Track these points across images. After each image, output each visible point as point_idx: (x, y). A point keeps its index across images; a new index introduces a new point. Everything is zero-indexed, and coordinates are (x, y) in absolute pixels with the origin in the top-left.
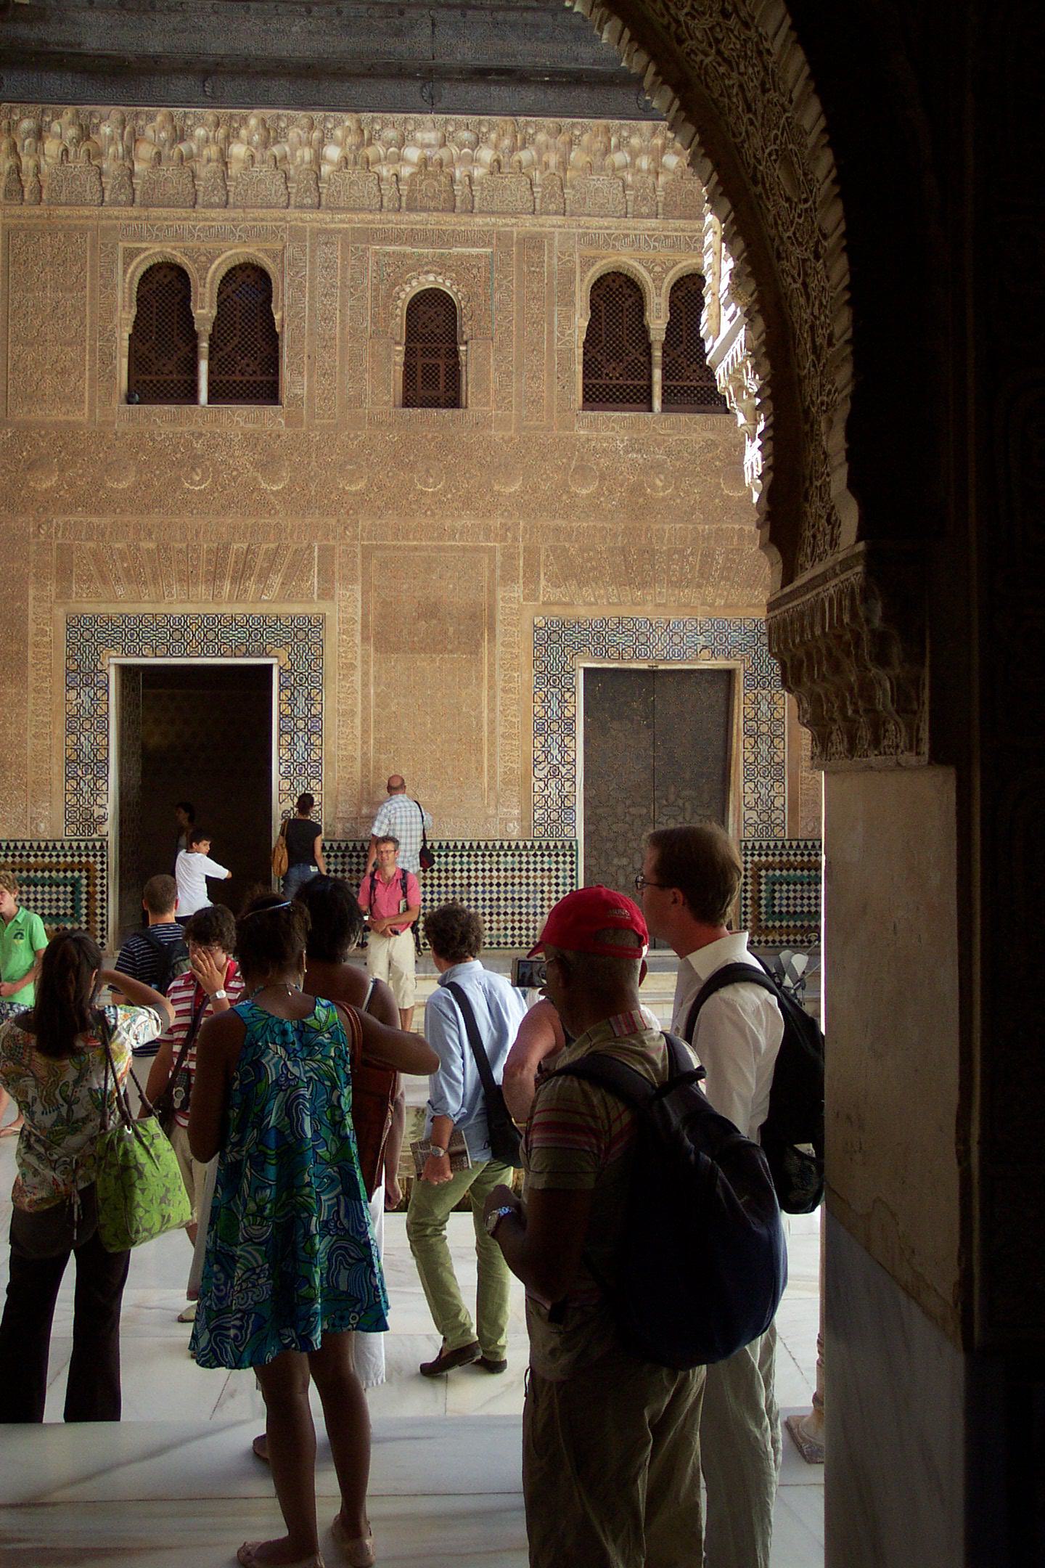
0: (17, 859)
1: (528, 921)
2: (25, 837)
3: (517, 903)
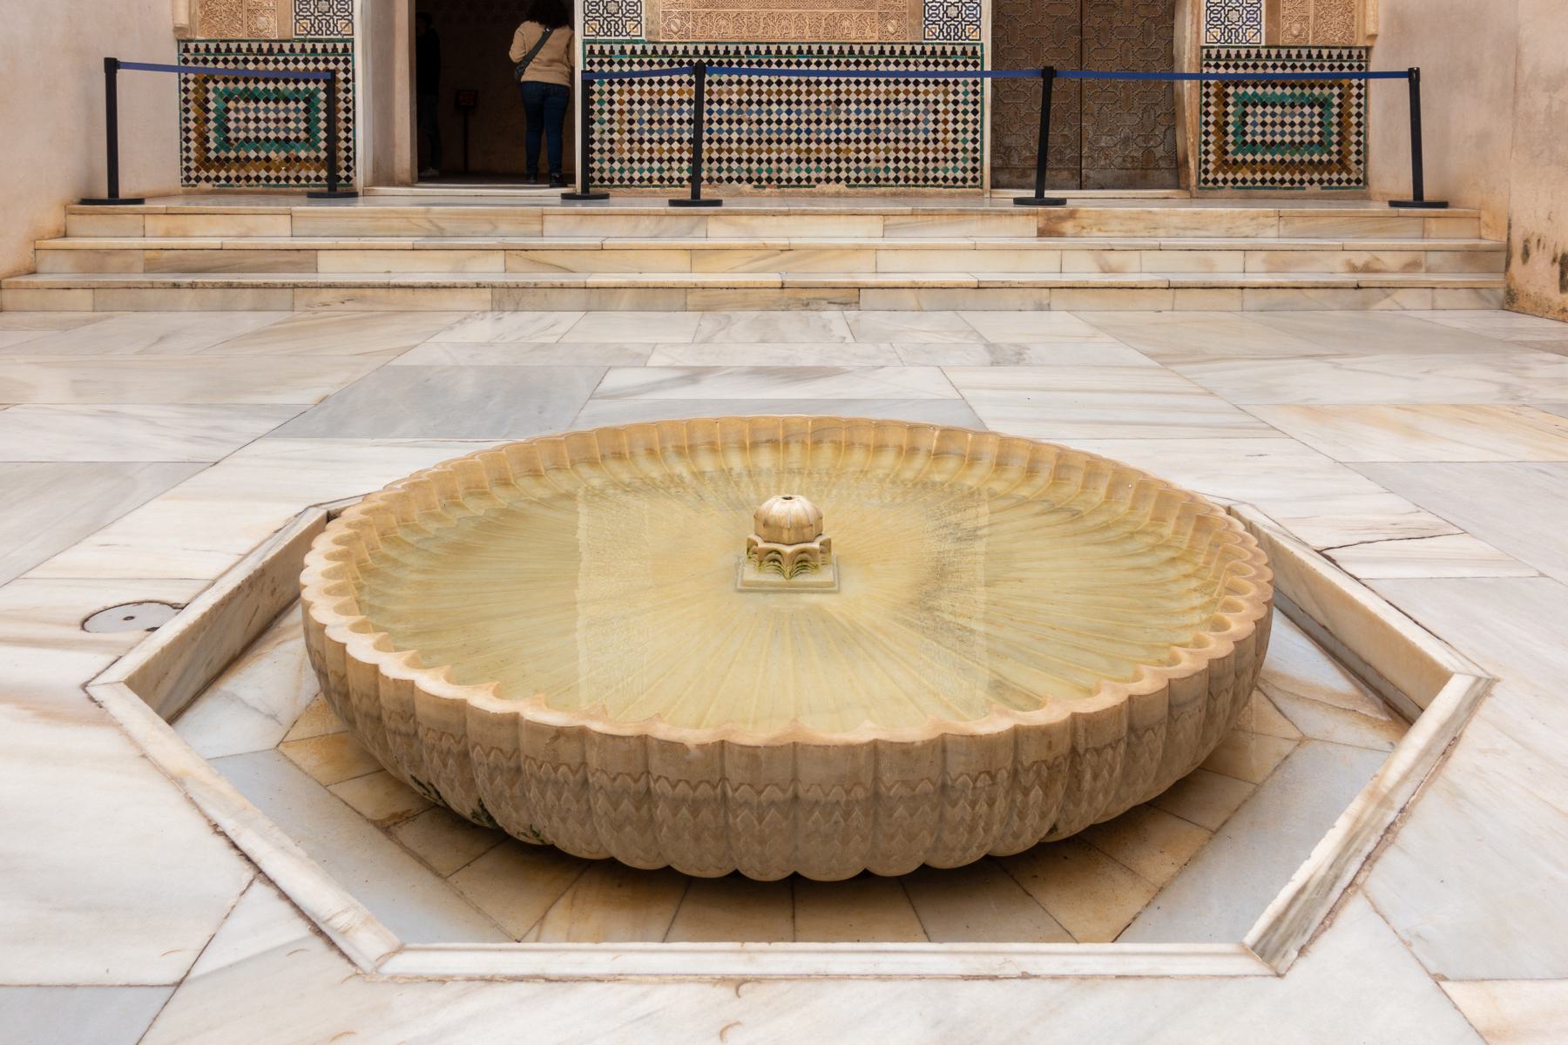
0: (231, 66)
1: (916, 151)
2: (240, 36)
3: (902, 126)
